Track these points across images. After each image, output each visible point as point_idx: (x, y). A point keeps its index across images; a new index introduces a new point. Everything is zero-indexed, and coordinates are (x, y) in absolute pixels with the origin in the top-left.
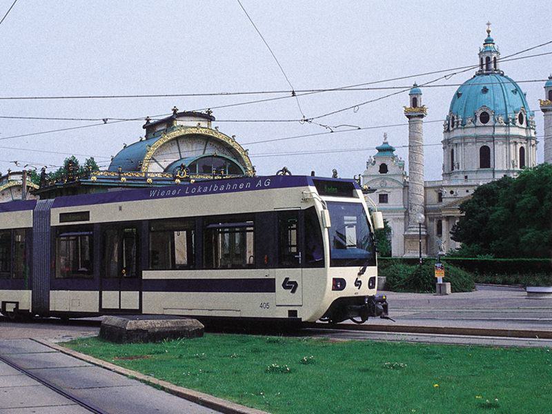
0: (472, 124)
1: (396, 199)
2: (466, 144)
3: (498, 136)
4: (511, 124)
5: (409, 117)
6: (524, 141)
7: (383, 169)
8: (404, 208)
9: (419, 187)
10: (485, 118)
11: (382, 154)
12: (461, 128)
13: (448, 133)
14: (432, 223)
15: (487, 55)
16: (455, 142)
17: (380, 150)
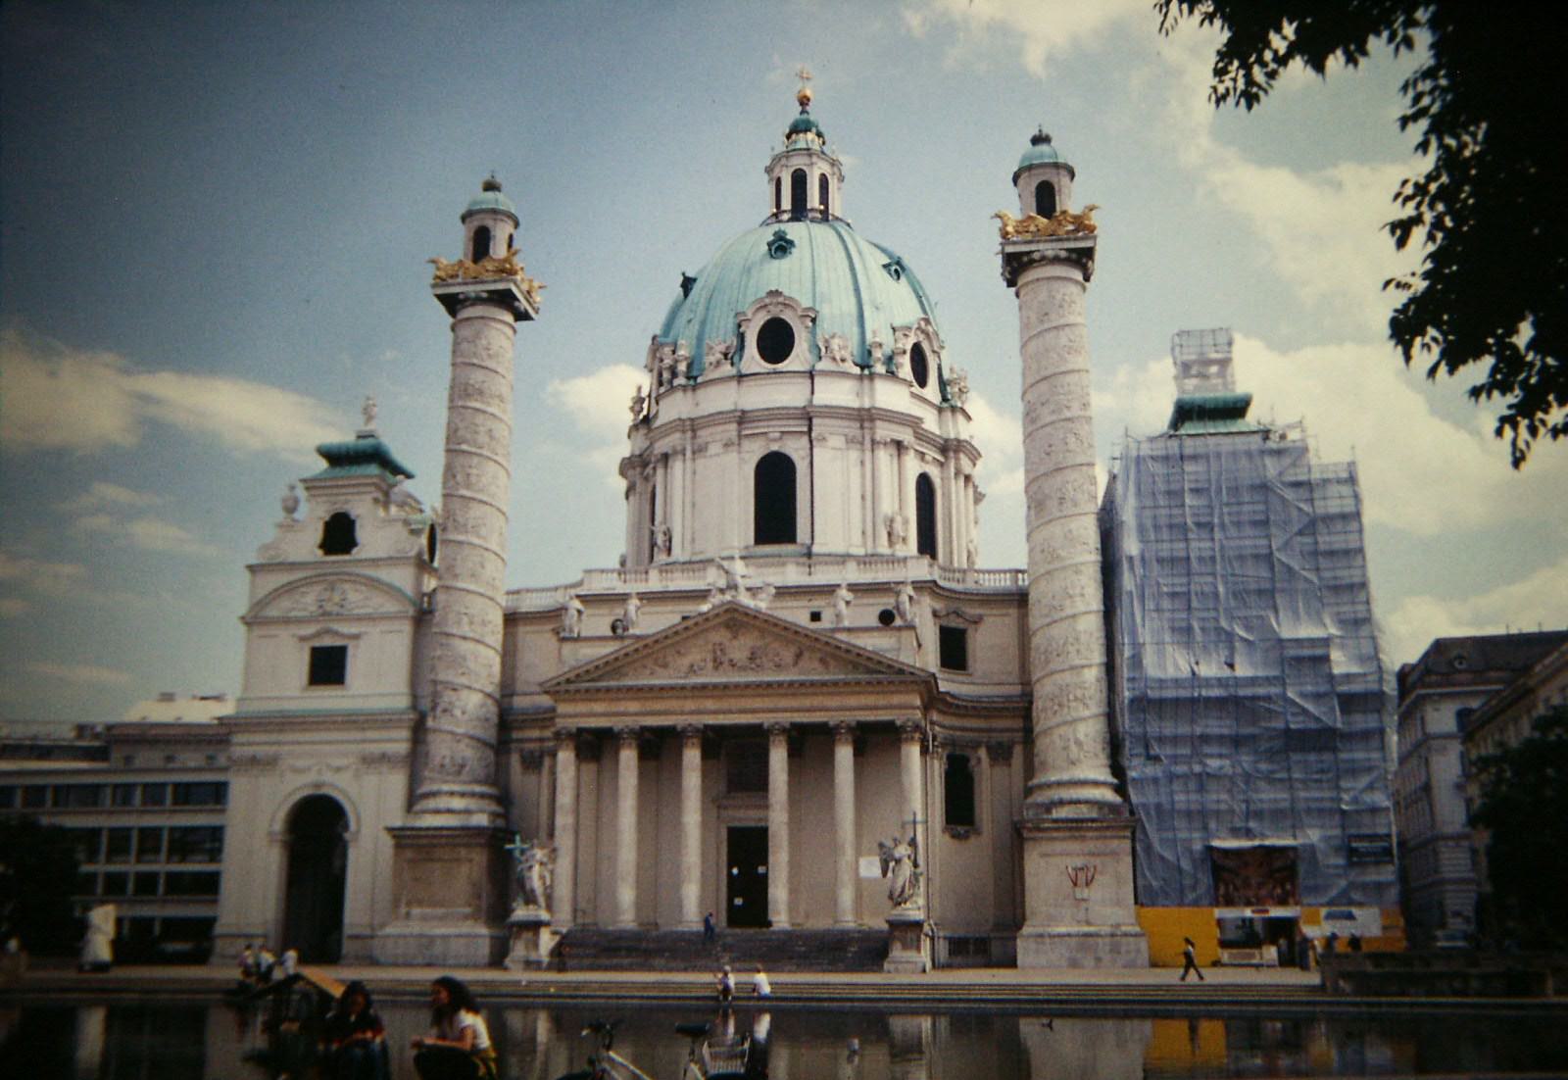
0: (727, 369)
1: (378, 674)
2: (699, 451)
3: (834, 412)
4: (880, 368)
5: (452, 303)
6: (932, 454)
7: (339, 535)
8: (414, 707)
9: (477, 605)
10: (776, 341)
11: (339, 471)
12: (684, 388)
13: (643, 431)
14: (533, 778)
15: (798, 162)
16: (662, 446)
17: (337, 458)
